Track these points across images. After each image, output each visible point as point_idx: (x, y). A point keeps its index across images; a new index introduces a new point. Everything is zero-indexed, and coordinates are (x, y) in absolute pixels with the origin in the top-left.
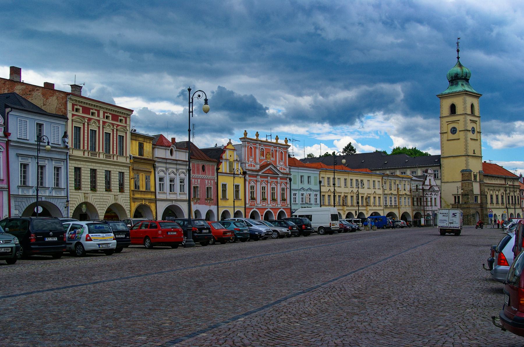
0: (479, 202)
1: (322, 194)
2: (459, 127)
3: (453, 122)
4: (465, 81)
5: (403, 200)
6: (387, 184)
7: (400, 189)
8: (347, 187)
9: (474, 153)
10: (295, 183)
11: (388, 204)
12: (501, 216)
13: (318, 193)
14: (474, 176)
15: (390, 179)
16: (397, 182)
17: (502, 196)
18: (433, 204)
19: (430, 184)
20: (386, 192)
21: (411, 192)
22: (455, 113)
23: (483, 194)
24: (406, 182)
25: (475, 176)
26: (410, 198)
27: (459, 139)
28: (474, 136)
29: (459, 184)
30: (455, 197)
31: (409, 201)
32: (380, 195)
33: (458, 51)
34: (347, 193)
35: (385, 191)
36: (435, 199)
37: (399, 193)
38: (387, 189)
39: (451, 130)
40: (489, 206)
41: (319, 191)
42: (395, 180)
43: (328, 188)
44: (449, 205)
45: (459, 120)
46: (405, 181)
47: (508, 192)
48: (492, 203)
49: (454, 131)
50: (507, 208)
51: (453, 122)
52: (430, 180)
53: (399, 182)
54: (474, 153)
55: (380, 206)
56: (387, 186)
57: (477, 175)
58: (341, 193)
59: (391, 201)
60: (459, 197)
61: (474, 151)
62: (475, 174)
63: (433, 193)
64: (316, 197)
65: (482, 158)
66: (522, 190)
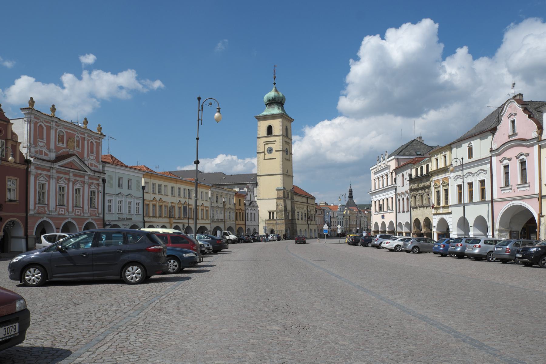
0: (290, 218)
1: (146, 202)
2: (275, 147)
4: (280, 105)
5: (228, 214)
6: (214, 195)
7: (226, 203)
8: (174, 197)
9: (287, 173)
10: (110, 186)
12: (304, 231)
13: (141, 201)
14: (287, 194)
15: (217, 192)
16: (224, 196)
17: (305, 213)
18: (253, 220)
19: (250, 199)
20: (213, 205)
21: (235, 207)
22: (272, 134)
23: (293, 211)
24: (231, 195)
25: (288, 194)
26: (234, 213)
30: (270, 213)
31: (233, 215)
32: (208, 207)
33: (275, 78)
34: (175, 203)
35: (212, 203)
36: (254, 214)
37: (225, 207)
38: (214, 202)
40: (297, 222)
41: (142, 198)
42: (222, 193)
43: (153, 196)
44: (264, 221)
45: (275, 141)
46: (230, 194)
47: (309, 210)
48: (298, 219)
49: (270, 150)
50: (308, 224)
52: (250, 195)
53: (225, 196)
54: (287, 173)
56: (214, 199)
57: (289, 193)
58: (168, 202)
60: (273, 213)
61: (287, 170)
62: (288, 192)
63: (253, 209)
64: (138, 206)
65: (292, 178)
66: (317, 209)
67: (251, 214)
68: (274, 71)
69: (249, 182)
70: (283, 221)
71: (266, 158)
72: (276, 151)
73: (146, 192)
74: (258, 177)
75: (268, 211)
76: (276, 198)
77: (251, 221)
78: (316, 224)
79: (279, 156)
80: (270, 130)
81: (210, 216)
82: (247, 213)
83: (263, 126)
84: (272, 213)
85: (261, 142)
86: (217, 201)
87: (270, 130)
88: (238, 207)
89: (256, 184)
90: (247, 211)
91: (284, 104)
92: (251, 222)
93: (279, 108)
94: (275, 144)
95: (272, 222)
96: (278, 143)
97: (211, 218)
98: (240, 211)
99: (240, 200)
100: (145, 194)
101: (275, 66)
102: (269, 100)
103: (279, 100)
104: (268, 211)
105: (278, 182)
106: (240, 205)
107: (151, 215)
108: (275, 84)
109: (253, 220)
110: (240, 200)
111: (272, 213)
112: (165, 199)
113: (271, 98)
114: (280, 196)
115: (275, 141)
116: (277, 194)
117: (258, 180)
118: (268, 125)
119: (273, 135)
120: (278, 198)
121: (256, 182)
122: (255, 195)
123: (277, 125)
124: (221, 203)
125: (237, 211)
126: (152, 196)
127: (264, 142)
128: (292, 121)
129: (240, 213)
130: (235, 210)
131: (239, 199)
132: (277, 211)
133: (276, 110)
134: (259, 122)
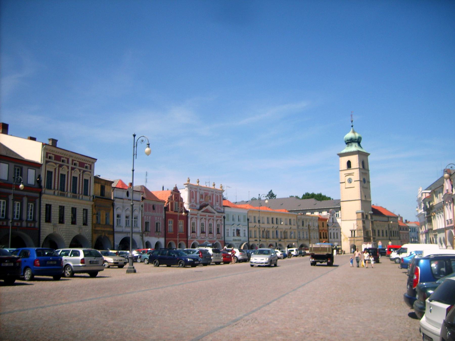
3: (349, 174)
4: (357, 143)
8: (269, 224)
11: (302, 236)
18: (336, 237)
22: (350, 167)
27: (354, 187)
28: (365, 185)
29: (355, 222)
30: (352, 232)
32: (295, 229)
34: (270, 228)
36: (337, 233)
39: (348, 180)
45: (354, 173)
49: (350, 181)
51: (349, 174)
55: (295, 238)
59: (303, 235)
60: (354, 232)
67: (334, 233)
68: (352, 116)
69: (334, 207)
70: (363, 238)
71: (346, 187)
72: (355, 181)
73: (249, 222)
74: (341, 203)
75: (350, 230)
76: (356, 219)
77: (334, 238)
78: (400, 239)
79: (357, 185)
80: (349, 164)
81: (297, 237)
82: (330, 233)
83: (344, 160)
84: (353, 232)
85: (342, 174)
86: (303, 225)
87: (349, 164)
88: (321, 228)
89: (340, 209)
90: (329, 231)
91: (360, 142)
92: (334, 239)
93: (356, 146)
94: (353, 175)
95: (353, 239)
96: (356, 175)
97: (298, 237)
98: (324, 231)
99: (323, 223)
100: (249, 224)
101: (352, 112)
102: (348, 140)
103: (355, 140)
104: (350, 230)
105: (357, 206)
106: (323, 226)
107: (253, 236)
108: (352, 126)
109: (336, 237)
110: (323, 223)
111: (353, 232)
112: (262, 225)
113: (349, 139)
114: (360, 218)
115: (354, 173)
116: (357, 216)
117: (341, 205)
118: (347, 162)
119: (352, 168)
120: (358, 219)
121: (339, 207)
122: (340, 217)
123: (355, 160)
124: (306, 226)
125: (320, 231)
126: (254, 224)
127: (345, 174)
128: (368, 155)
129: (323, 233)
130: (319, 230)
131: (322, 222)
132: (357, 231)
133: (354, 148)
134: (340, 158)
